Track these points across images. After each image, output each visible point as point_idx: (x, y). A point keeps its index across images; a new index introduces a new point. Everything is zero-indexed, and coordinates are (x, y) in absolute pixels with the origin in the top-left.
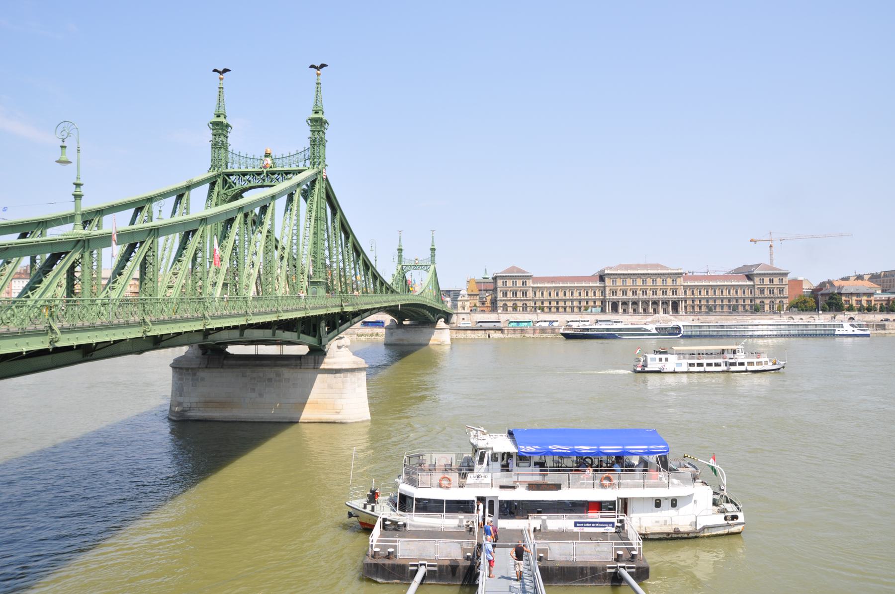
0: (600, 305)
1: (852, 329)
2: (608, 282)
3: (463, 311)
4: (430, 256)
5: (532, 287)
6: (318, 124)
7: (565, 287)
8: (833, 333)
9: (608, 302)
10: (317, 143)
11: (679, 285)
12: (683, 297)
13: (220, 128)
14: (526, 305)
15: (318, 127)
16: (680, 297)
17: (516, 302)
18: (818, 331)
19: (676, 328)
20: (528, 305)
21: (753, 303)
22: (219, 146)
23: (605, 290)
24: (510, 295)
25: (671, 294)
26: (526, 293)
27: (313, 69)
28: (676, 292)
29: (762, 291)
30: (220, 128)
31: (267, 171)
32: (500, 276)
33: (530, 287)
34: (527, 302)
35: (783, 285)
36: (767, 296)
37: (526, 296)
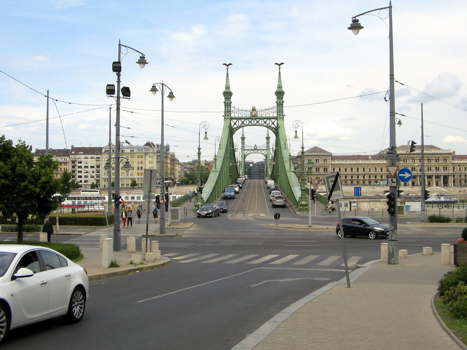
0: (386, 178)
4: (266, 143)
5: (332, 164)
6: (280, 94)
10: (280, 104)
11: (448, 163)
12: (452, 172)
13: (228, 95)
15: (281, 96)
16: (450, 172)
22: (228, 104)
25: (442, 170)
26: (327, 169)
27: (276, 65)
28: (446, 168)
30: (228, 95)
31: (255, 118)
33: (330, 164)
37: (327, 171)
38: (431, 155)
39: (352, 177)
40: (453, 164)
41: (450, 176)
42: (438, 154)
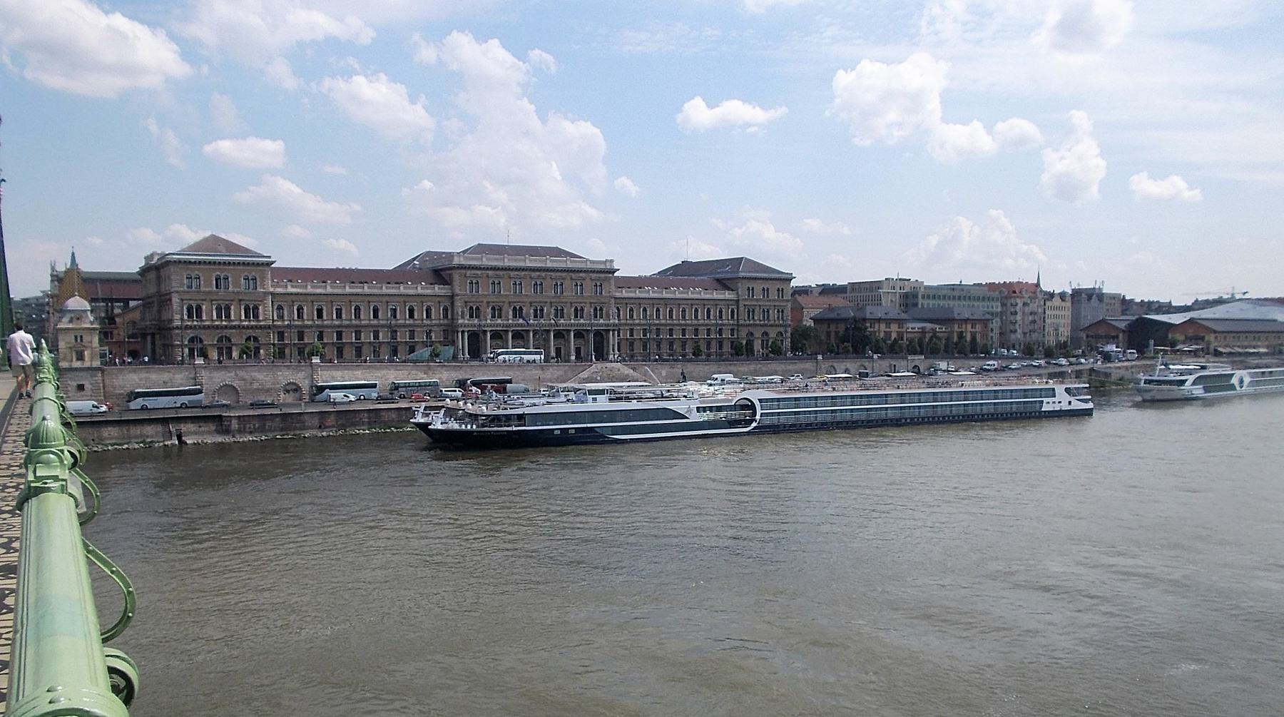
1: (1068, 398)
2: (460, 286)
3: (77, 364)
5: (273, 294)
7: (357, 295)
8: (1038, 408)
9: (463, 332)
14: (256, 339)
16: (611, 321)
17: (228, 332)
18: (1014, 406)
19: (743, 407)
20: (262, 340)
21: (735, 336)
23: (452, 303)
24: (209, 315)
26: (256, 308)
29: (751, 312)
32: (180, 262)
34: (258, 333)
35: (783, 301)
36: (758, 322)
38: (564, 274)
39: (340, 335)
40: (618, 300)
41: (611, 333)
42: (581, 271)
